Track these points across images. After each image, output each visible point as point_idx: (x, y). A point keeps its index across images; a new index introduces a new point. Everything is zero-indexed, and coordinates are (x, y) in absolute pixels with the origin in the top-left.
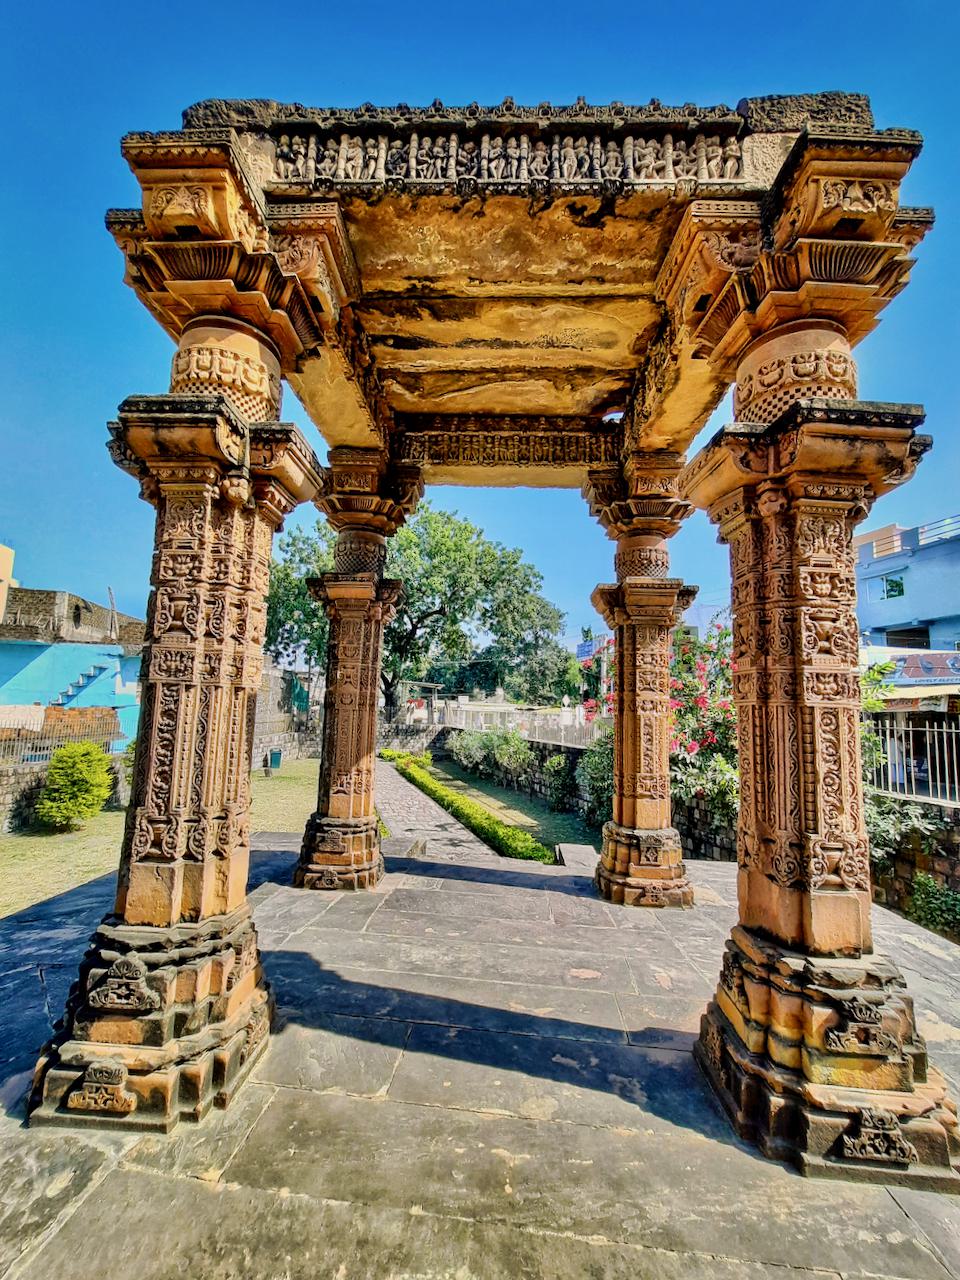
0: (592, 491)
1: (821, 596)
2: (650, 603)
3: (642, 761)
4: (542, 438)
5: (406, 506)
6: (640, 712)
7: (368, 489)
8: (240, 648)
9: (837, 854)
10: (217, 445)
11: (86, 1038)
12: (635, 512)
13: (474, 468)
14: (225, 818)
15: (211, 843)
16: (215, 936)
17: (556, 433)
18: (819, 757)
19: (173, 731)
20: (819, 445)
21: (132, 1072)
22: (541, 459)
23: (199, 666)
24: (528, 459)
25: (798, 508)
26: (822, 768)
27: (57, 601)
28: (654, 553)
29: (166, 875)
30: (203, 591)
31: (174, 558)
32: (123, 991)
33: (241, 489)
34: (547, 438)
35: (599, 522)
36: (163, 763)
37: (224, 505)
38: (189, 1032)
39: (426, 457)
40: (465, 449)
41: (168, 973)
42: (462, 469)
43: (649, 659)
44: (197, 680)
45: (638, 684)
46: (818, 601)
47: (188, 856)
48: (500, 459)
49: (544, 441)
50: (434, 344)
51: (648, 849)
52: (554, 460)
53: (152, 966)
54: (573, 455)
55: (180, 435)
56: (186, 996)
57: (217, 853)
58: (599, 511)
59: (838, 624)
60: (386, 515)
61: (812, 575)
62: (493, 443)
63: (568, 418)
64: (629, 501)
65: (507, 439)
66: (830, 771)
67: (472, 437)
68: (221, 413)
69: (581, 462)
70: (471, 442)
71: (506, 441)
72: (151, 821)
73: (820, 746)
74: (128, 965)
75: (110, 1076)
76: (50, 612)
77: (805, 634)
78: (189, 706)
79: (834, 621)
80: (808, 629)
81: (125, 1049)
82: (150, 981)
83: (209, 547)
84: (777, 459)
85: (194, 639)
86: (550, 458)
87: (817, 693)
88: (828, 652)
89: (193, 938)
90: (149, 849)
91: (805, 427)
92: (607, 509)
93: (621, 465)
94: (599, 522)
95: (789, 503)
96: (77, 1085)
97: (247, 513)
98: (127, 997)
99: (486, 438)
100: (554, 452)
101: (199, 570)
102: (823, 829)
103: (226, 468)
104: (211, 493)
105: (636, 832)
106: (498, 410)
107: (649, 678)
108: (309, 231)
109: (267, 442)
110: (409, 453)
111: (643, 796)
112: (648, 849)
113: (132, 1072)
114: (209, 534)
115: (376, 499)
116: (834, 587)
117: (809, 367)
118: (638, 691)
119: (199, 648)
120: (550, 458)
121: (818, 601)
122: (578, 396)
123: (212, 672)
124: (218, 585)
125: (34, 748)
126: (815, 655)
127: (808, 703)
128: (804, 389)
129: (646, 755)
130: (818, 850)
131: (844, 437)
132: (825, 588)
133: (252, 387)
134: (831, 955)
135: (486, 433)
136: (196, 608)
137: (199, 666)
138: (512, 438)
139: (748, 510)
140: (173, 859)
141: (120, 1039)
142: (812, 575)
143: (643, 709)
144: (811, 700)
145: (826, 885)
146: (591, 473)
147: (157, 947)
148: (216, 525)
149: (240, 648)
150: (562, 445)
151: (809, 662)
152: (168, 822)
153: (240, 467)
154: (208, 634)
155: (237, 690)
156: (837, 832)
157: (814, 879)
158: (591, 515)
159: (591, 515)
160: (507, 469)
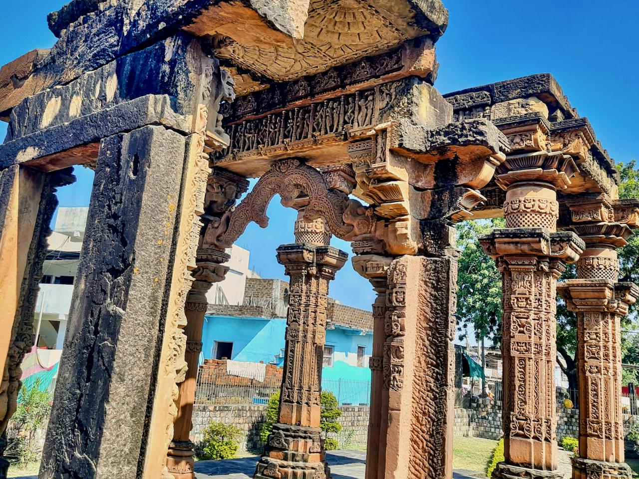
1: (521, 307)
2: (588, 296)
3: (591, 409)
6: (588, 374)
8: (315, 328)
9: (522, 422)
10: (304, 258)
11: (269, 456)
14: (310, 391)
15: (305, 400)
16: (305, 432)
18: (516, 378)
19: (293, 358)
20: (504, 247)
21: (280, 466)
23: (301, 334)
26: (517, 383)
27: (274, 287)
28: (595, 260)
29: (291, 407)
30: (302, 308)
31: (294, 296)
32: (278, 442)
33: (314, 270)
36: (290, 368)
37: (309, 277)
38: (296, 461)
41: (291, 439)
43: (594, 336)
44: (300, 339)
45: (586, 354)
46: (519, 310)
47: (298, 402)
50: (403, 181)
51: (592, 472)
53: (286, 436)
55: (293, 256)
56: (295, 449)
57: (307, 404)
59: (528, 320)
61: (517, 298)
66: (521, 385)
68: (304, 249)
72: (287, 389)
73: (517, 374)
74: (279, 433)
75: (275, 466)
76: (269, 295)
77: (512, 324)
78: (298, 347)
79: (527, 318)
80: (514, 322)
81: (278, 460)
82: (285, 440)
83: (304, 292)
85: (299, 325)
87: (518, 351)
88: (523, 332)
89: (298, 430)
90: (286, 398)
96: (266, 468)
97: (317, 278)
98: (279, 444)
101: (301, 300)
102: (517, 410)
103: (308, 265)
104: (304, 272)
105: (586, 461)
107: (594, 349)
109: (321, 253)
111: (592, 435)
112: (592, 472)
113: (280, 466)
114: (304, 287)
116: (527, 304)
117: (516, 206)
118: (586, 359)
119: (301, 328)
121: (519, 310)
123: (305, 336)
124: (307, 305)
125: (260, 394)
126: (517, 334)
127: (512, 355)
128: (515, 216)
129: (593, 406)
130: (515, 419)
131: (513, 243)
132: (523, 304)
133: (318, 231)
134: (517, 465)
136: (300, 314)
137: (301, 334)
140: (293, 402)
141: (277, 457)
142: (517, 298)
143: (590, 372)
144: (514, 353)
145: (517, 435)
147: (287, 430)
148: (306, 284)
149: (315, 328)
151: (513, 337)
152: (292, 389)
153: (312, 263)
154: (304, 323)
155: (314, 343)
156: (523, 412)
157: (512, 431)
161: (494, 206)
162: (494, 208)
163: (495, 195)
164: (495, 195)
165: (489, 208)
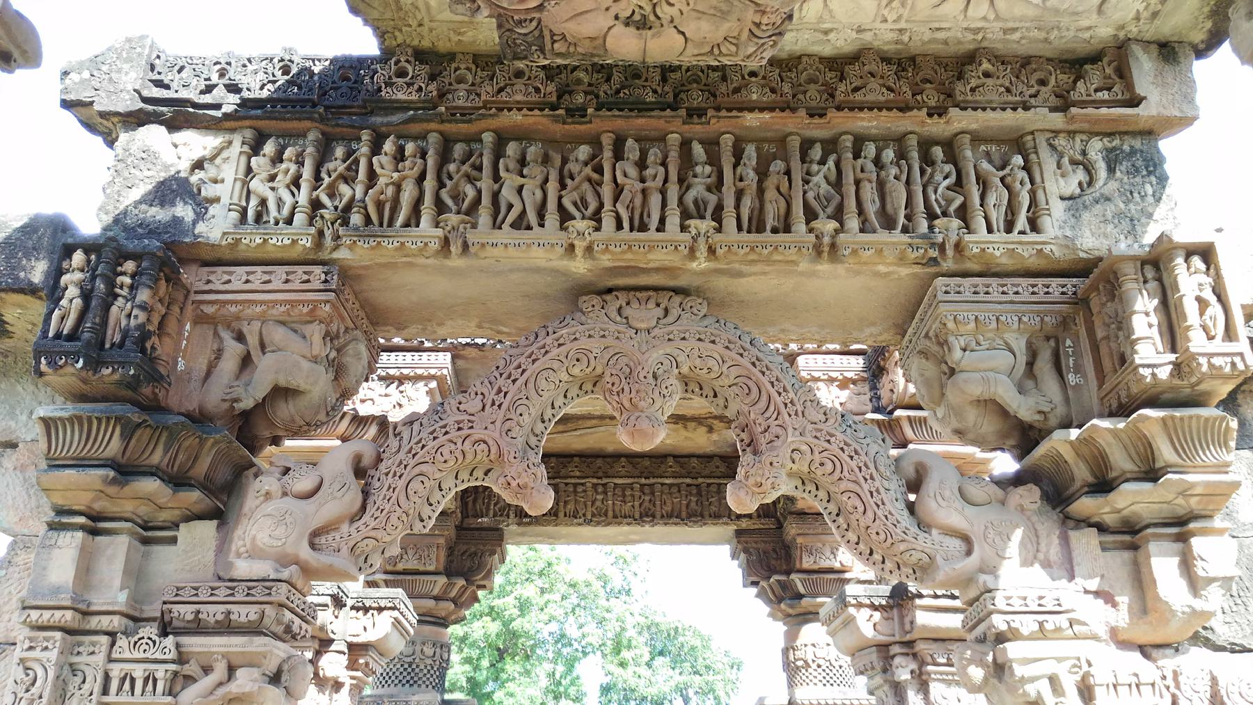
0: (743, 555)
4: (670, 486)
5: (482, 583)
7: (432, 568)
12: (802, 591)
13: (579, 529)
17: (688, 481)
22: (670, 516)
24: (653, 516)
25: (929, 674)
34: (678, 485)
35: (757, 596)
39: (512, 515)
40: (566, 502)
42: (563, 530)
48: (615, 517)
49: (674, 490)
52: (689, 516)
54: (713, 508)
58: (755, 584)
60: (454, 601)
62: (605, 493)
63: (708, 457)
64: (793, 576)
65: (624, 487)
67: (575, 485)
69: (725, 519)
70: (575, 492)
71: (624, 490)
84: (902, 624)
86: (684, 514)
91: (918, 602)
92: (763, 583)
93: (780, 526)
94: (757, 596)
95: (920, 669)
99: (595, 486)
100: (688, 506)
106: (610, 448)
108: (416, 379)
110: (488, 509)
115: (442, 580)
120: (684, 514)
122: (715, 437)
135: (595, 481)
138: (631, 486)
139: (885, 671)
146: (739, 533)
150: (699, 494)
158: (745, 586)
159: (745, 586)
160: (626, 528)
161: (629, 520)
162: (629, 524)
163: (633, 496)
164: (633, 496)
165: (619, 524)
